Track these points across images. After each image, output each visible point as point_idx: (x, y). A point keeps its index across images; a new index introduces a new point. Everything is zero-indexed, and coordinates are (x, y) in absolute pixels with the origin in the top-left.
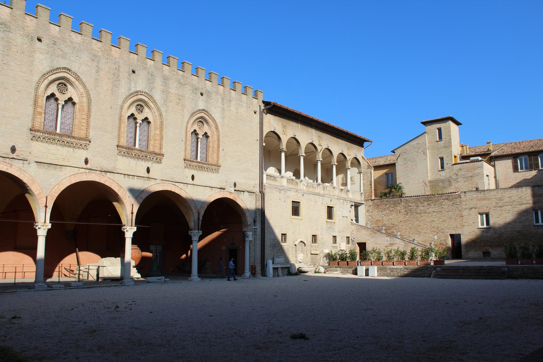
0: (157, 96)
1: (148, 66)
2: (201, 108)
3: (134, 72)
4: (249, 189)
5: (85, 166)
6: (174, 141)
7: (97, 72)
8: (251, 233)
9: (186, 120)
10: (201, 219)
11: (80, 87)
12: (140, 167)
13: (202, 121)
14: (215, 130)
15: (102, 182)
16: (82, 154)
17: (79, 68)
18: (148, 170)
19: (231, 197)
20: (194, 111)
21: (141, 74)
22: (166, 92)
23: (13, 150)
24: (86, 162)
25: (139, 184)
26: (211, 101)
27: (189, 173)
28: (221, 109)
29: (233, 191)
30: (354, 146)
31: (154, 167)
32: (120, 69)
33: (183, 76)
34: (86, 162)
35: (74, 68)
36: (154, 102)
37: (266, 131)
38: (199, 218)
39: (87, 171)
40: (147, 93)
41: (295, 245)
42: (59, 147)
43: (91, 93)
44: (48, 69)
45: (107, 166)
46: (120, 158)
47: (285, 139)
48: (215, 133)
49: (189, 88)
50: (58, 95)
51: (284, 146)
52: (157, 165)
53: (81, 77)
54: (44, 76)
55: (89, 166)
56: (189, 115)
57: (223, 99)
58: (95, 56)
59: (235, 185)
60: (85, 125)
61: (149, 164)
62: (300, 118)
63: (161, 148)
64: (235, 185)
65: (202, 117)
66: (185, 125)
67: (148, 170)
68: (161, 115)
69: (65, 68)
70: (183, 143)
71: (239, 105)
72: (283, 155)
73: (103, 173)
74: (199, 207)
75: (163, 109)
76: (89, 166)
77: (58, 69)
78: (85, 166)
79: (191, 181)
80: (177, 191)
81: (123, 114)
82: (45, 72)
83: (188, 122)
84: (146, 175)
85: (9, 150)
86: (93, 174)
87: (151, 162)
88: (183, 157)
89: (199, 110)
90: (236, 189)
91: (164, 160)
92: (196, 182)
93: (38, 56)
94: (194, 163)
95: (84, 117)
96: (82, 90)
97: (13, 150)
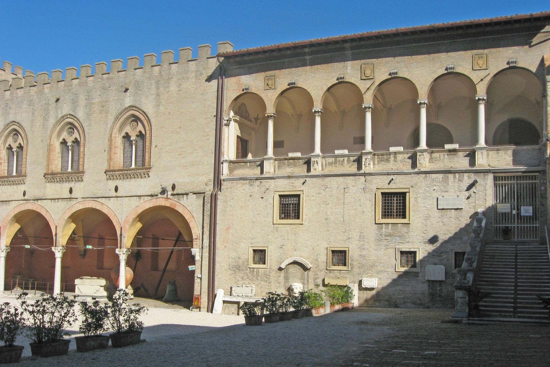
0: (81, 114)
1: (74, 86)
2: (127, 105)
4: (195, 191)
5: (23, 198)
7: (33, 113)
9: (109, 126)
12: (62, 189)
15: (34, 209)
16: (22, 188)
17: (21, 117)
18: (71, 191)
19: (167, 204)
20: (119, 112)
22: (89, 105)
24: (24, 194)
26: (139, 92)
27: (112, 184)
28: (154, 97)
30: (398, 59)
32: (50, 103)
33: (108, 78)
34: (24, 194)
37: (230, 95)
39: (25, 202)
40: (70, 115)
41: (280, 269)
42: (9, 187)
43: (28, 134)
44: (3, 128)
45: (38, 193)
46: (48, 185)
47: (270, 99)
49: (114, 88)
51: (270, 110)
52: (80, 183)
55: (26, 197)
57: (157, 83)
58: (31, 101)
59: (174, 187)
61: (72, 185)
62: (306, 50)
66: (108, 132)
67: (71, 191)
70: (106, 153)
71: (183, 78)
73: (36, 202)
74: (122, 222)
75: (85, 125)
76: (26, 197)
77: (8, 124)
79: (114, 194)
80: (98, 207)
81: (52, 143)
83: (112, 128)
86: (28, 204)
87: (74, 182)
89: (126, 109)
90: (175, 192)
91: (86, 177)
92: (120, 193)
94: (117, 172)
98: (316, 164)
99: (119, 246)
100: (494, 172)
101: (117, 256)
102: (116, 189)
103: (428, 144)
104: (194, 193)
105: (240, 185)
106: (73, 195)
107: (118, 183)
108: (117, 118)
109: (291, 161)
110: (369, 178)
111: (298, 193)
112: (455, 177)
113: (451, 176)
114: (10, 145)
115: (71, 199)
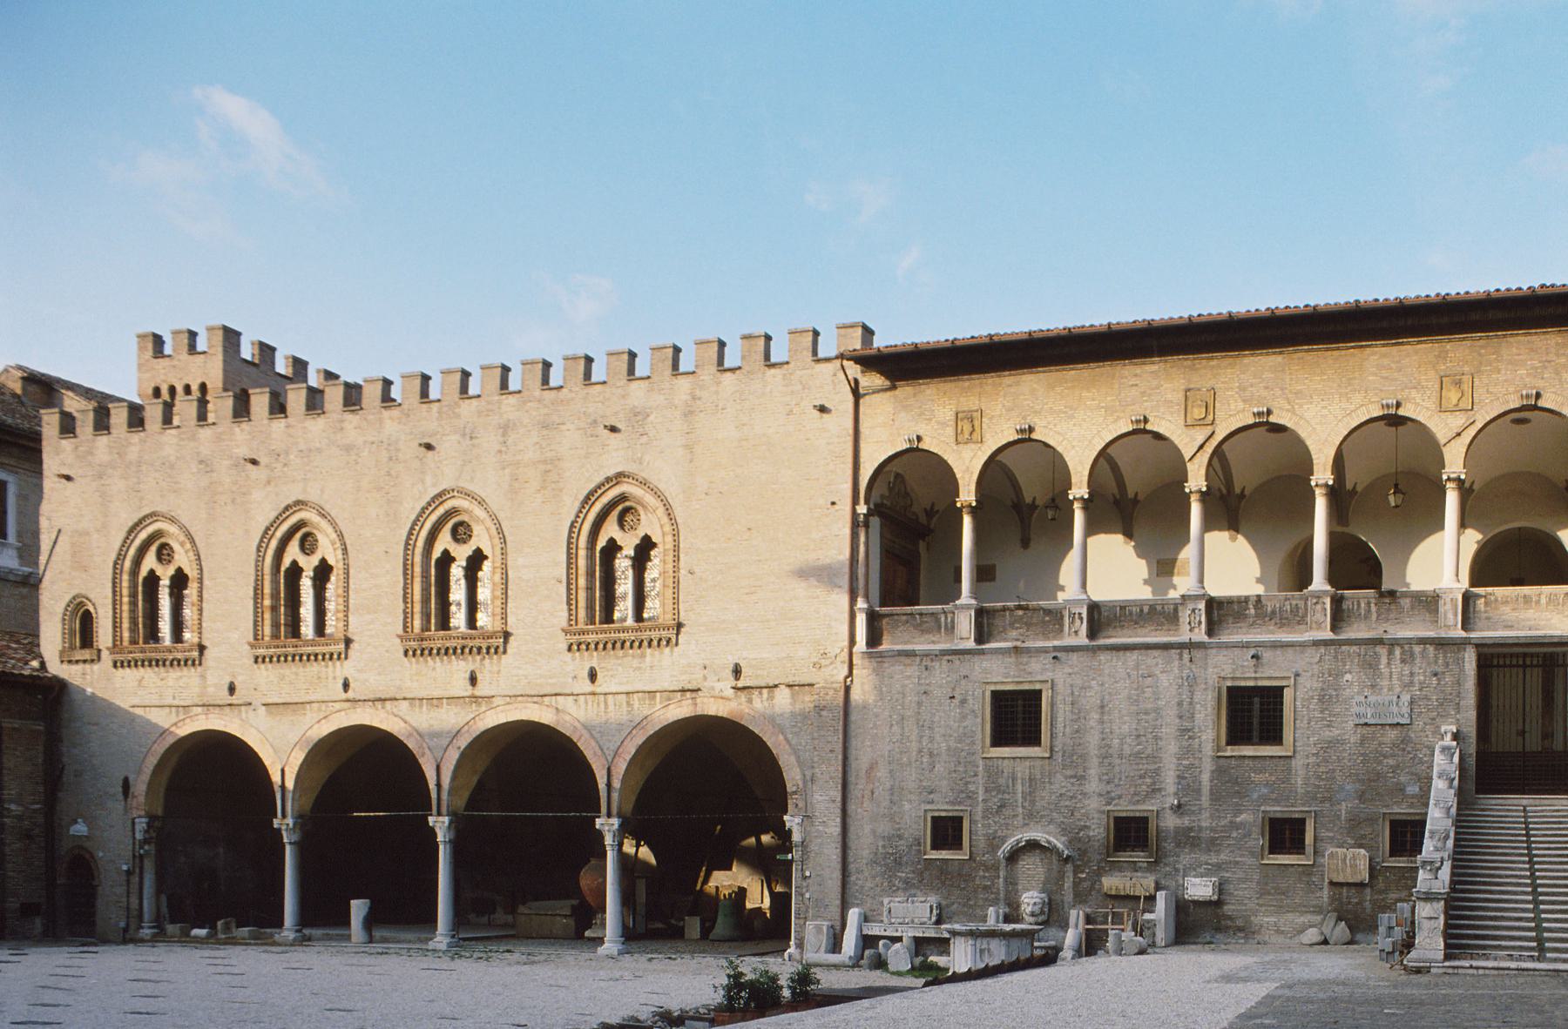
2: (611, 472)
3: (429, 447)
4: (790, 680)
5: (344, 696)
6: (532, 584)
8: (798, 820)
10: (617, 784)
11: (330, 530)
13: (624, 510)
14: (665, 520)
15: (376, 724)
18: (473, 680)
20: (592, 486)
21: (448, 445)
23: (232, 689)
24: (346, 686)
25: (449, 718)
29: (730, 693)
31: (488, 668)
34: (346, 686)
35: (312, 495)
36: (482, 502)
38: (609, 785)
39: (347, 705)
44: (274, 514)
48: (668, 528)
50: (303, 561)
53: (327, 507)
54: (267, 533)
55: (350, 694)
56: (577, 505)
59: (737, 672)
60: (341, 608)
63: (504, 617)
64: (737, 672)
65: (623, 498)
67: (473, 680)
68: (500, 531)
69: (298, 503)
72: (967, 522)
73: (379, 704)
76: (350, 694)
77: (287, 508)
78: (344, 696)
79: (587, 686)
82: (267, 523)
84: (469, 691)
85: (226, 692)
88: (564, 624)
89: (608, 480)
90: (740, 684)
93: (257, 495)
95: (340, 591)
96: (334, 536)
97: (232, 689)
98: (1078, 622)
99: (604, 809)
100: (1477, 646)
101: (600, 836)
102: (593, 676)
103: (1332, 578)
104: (789, 686)
105: (898, 668)
106: (482, 689)
107: (594, 659)
108: (588, 500)
109: (1020, 613)
110: (1197, 654)
111: (1038, 687)
112: (1390, 653)
113: (1382, 651)
114: (294, 563)
115: (475, 699)
